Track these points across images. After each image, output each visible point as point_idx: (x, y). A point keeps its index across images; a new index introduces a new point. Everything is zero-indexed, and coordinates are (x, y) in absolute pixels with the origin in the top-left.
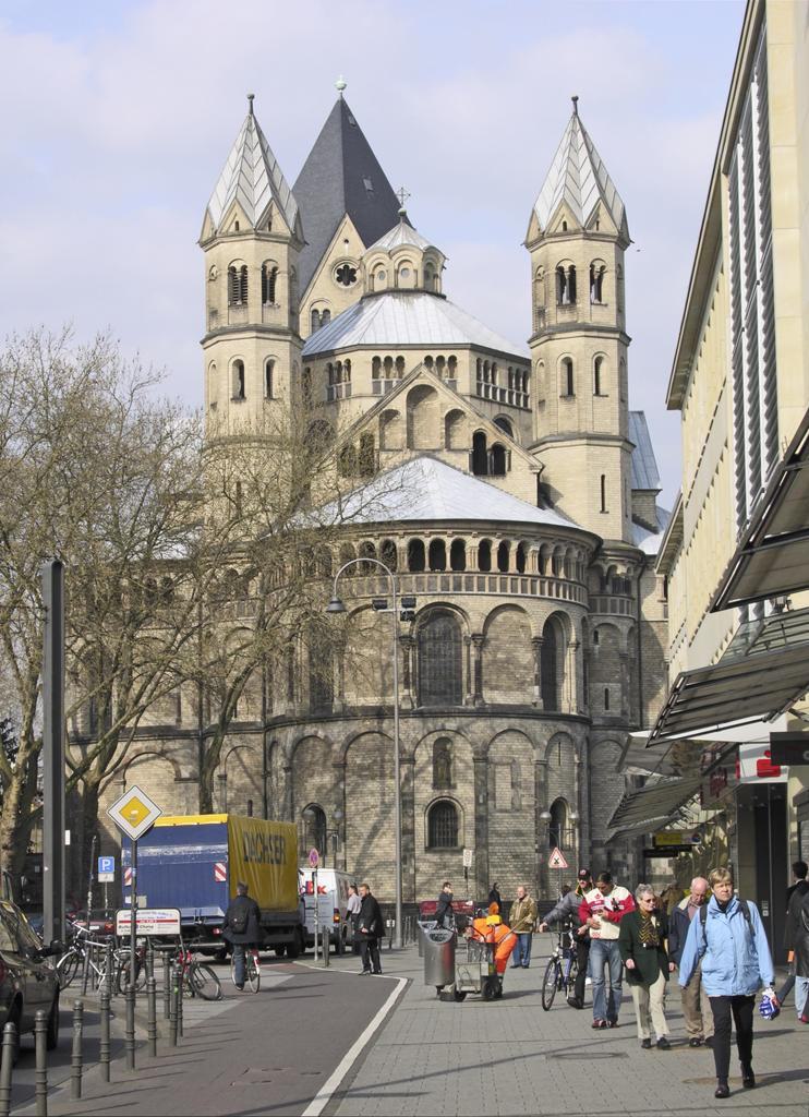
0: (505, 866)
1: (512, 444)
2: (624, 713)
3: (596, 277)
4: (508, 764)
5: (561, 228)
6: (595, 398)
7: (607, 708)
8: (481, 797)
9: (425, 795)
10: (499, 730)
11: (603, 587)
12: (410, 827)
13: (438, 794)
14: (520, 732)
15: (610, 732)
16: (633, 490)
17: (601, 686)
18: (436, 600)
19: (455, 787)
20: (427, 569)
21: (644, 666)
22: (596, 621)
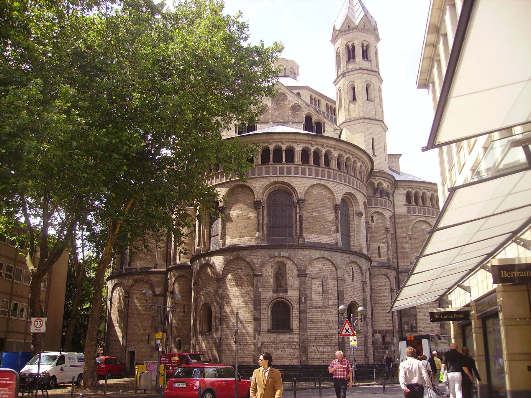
0: (319, 342)
1: (325, 119)
2: (389, 260)
3: (365, 49)
4: (320, 278)
5: (347, 28)
6: (367, 101)
7: (380, 257)
8: (303, 298)
9: (268, 297)
10: (314, 257)
11: (375, 194)
12: (258, 317)
13: (275, 295)
14: (327, 259)
15: (382, 269)
16: (388, 155)
17: (376, 245)
18: (276, 179)
19: (286, 291)
20: (271, 162)
21: (398, 238)
22: (372, 210)
